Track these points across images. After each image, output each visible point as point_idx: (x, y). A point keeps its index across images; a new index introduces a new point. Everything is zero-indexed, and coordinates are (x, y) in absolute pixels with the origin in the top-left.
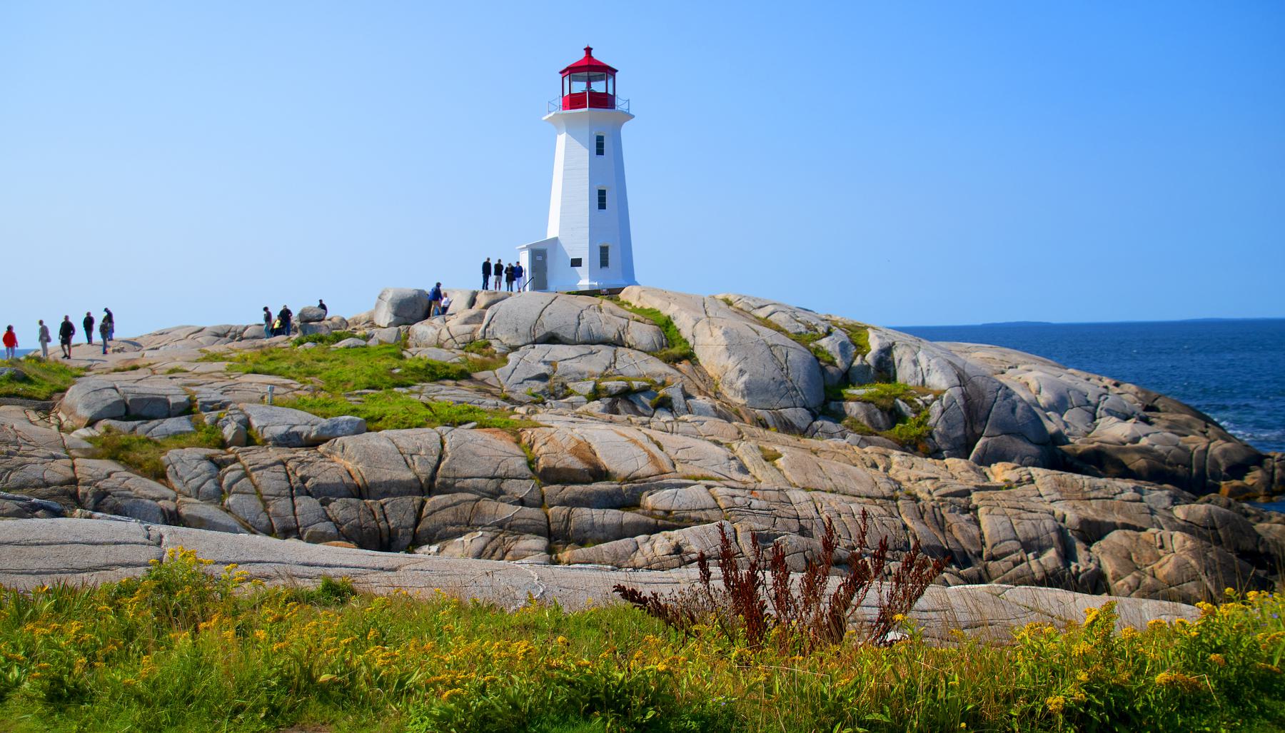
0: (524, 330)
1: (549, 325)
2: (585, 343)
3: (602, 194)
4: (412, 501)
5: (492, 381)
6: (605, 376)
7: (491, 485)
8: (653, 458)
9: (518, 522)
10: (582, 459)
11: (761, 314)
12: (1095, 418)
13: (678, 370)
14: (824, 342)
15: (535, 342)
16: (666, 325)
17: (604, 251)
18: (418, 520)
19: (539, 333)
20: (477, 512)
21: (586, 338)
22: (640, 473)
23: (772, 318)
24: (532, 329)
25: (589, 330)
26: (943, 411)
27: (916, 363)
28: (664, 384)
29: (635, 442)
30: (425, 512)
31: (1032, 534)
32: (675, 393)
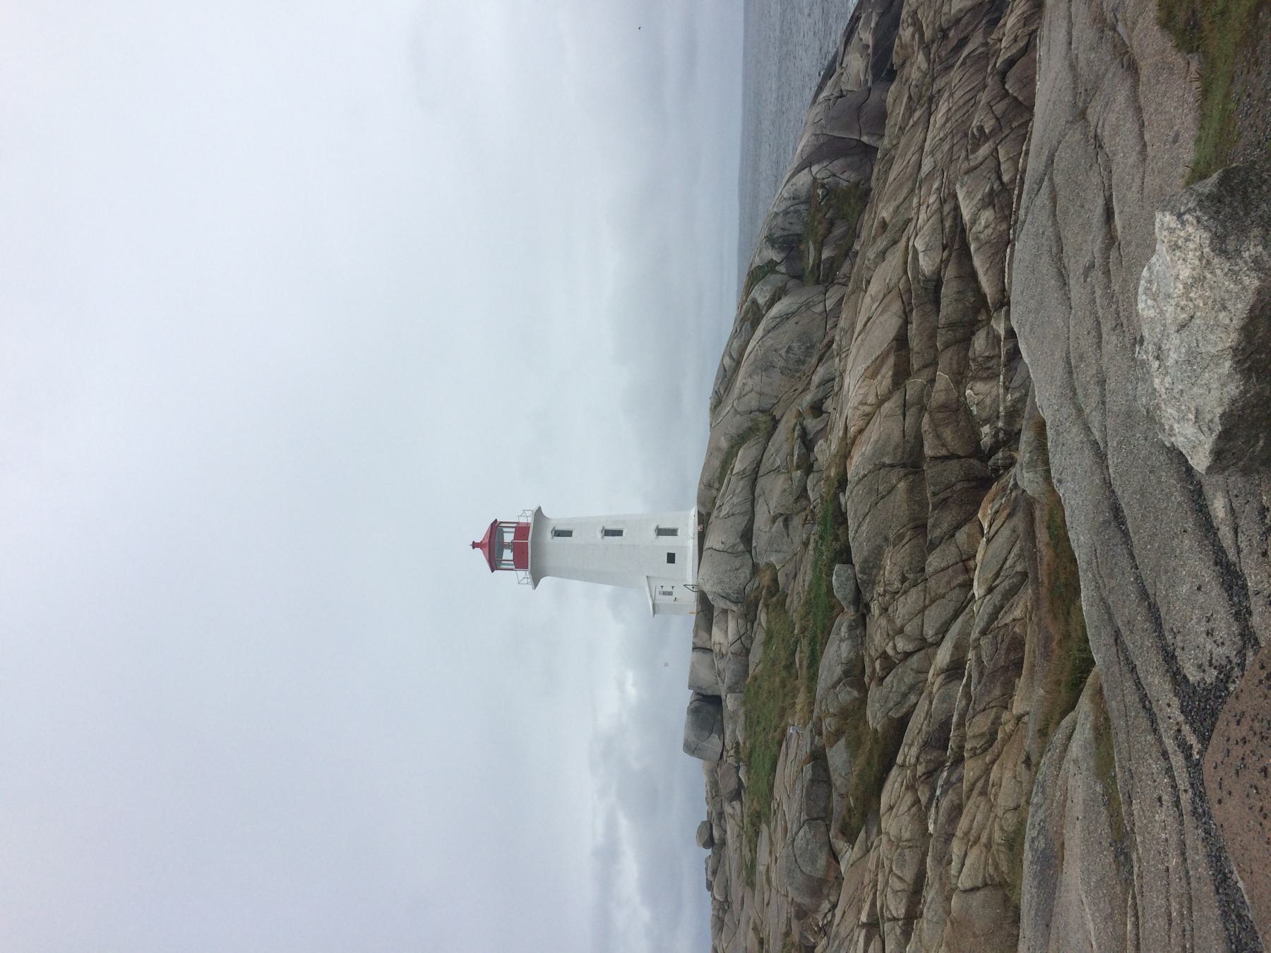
0: (737, 562)
2: (753, 506)
3: (608, 533)
4: (929, 471)
5: (790, 567)
7: (912, 411)
9: (955, 366)
15: (750, 552)
16: (739, 441)
17: (661, 532)
18: (951, 456)
19: (741, 547)
20: (943, 407)
21: (748, 505)
22: (900, 313)
23: (735, 355)
24: (736, 554)
25: (739, 504)
26: (834, 175)
27: (786, 213)
28: (800, 414)
30: (944, 452)
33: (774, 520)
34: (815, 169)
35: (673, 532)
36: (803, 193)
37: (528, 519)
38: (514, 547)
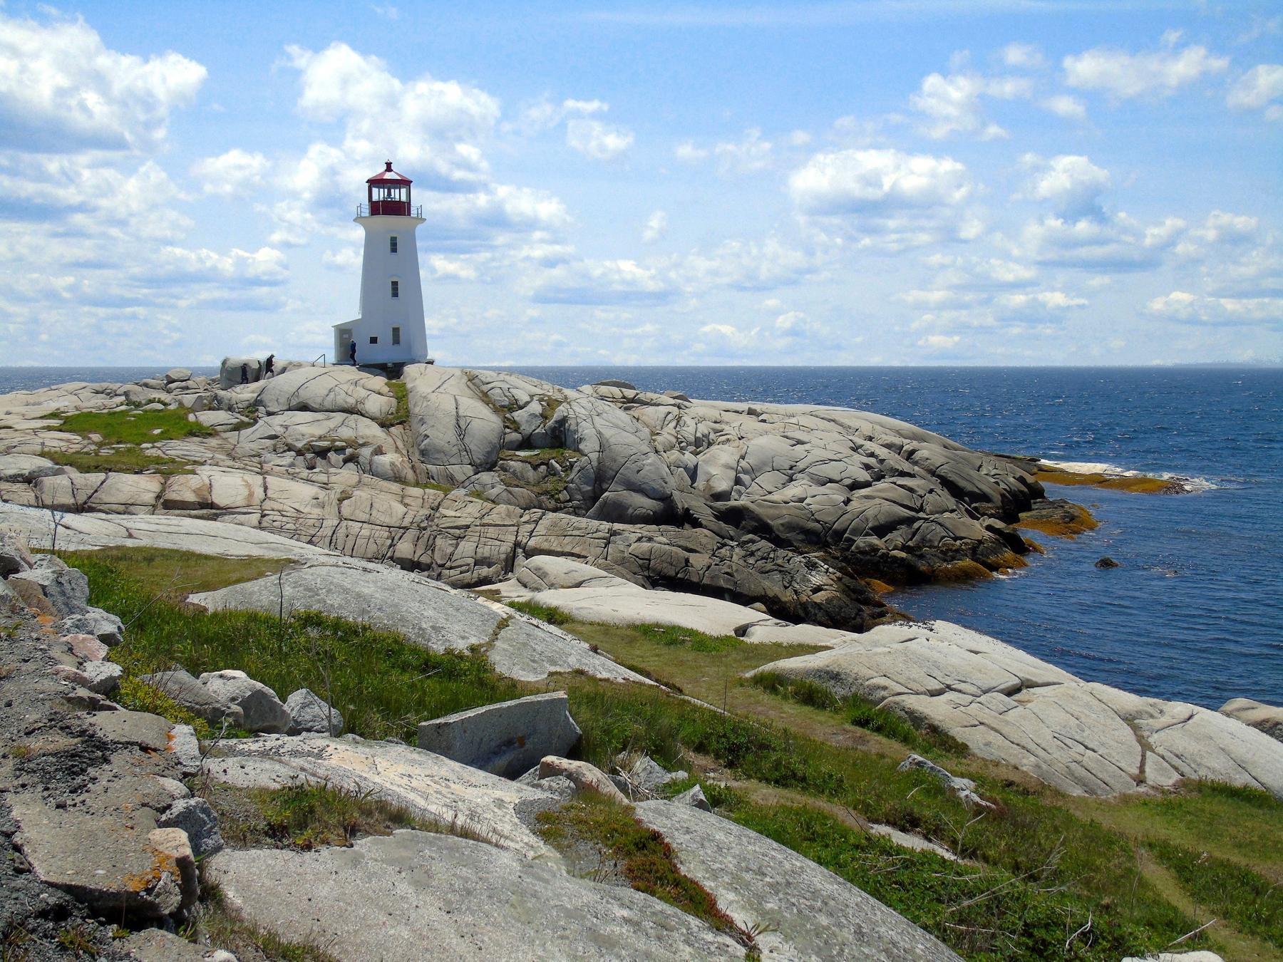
0: (282, 400)
1: (305, 395)
6: (320, 438)
8: (251, 495)
10: (198, 495)
11: (485, 388)
12: (791, 480)
13: (389, 433)
14: (518, 415)
15: (289, 410)
19: (294, 403)
29: (248, 485)
31: (487, 554)
32: (366, 452)
33: (286, 427)
34: (594, 456)
35: (396, 341)
36: (581, 446)
37: (414, 212)
38: (389, 202)
